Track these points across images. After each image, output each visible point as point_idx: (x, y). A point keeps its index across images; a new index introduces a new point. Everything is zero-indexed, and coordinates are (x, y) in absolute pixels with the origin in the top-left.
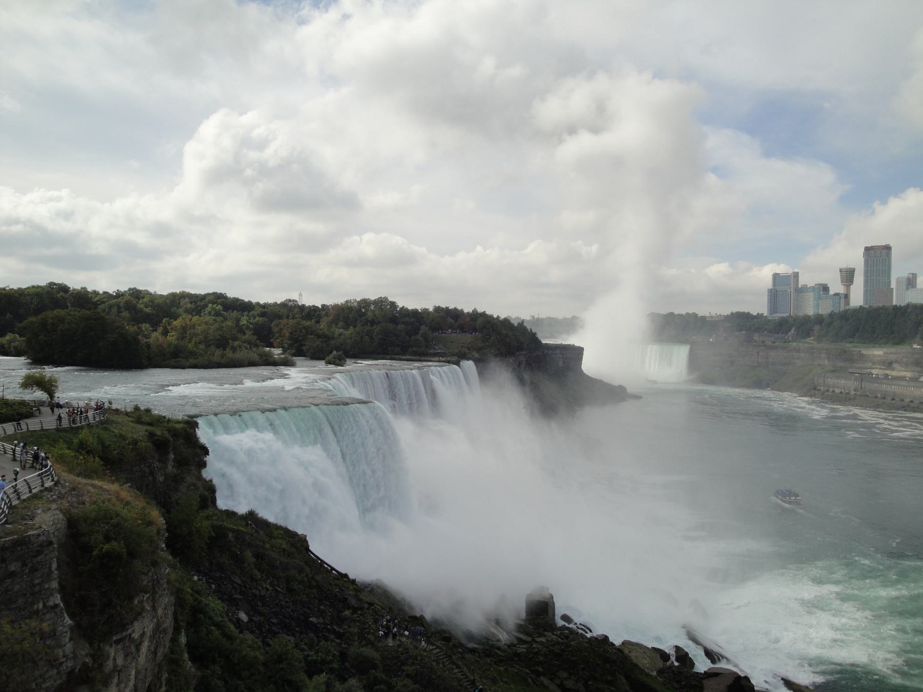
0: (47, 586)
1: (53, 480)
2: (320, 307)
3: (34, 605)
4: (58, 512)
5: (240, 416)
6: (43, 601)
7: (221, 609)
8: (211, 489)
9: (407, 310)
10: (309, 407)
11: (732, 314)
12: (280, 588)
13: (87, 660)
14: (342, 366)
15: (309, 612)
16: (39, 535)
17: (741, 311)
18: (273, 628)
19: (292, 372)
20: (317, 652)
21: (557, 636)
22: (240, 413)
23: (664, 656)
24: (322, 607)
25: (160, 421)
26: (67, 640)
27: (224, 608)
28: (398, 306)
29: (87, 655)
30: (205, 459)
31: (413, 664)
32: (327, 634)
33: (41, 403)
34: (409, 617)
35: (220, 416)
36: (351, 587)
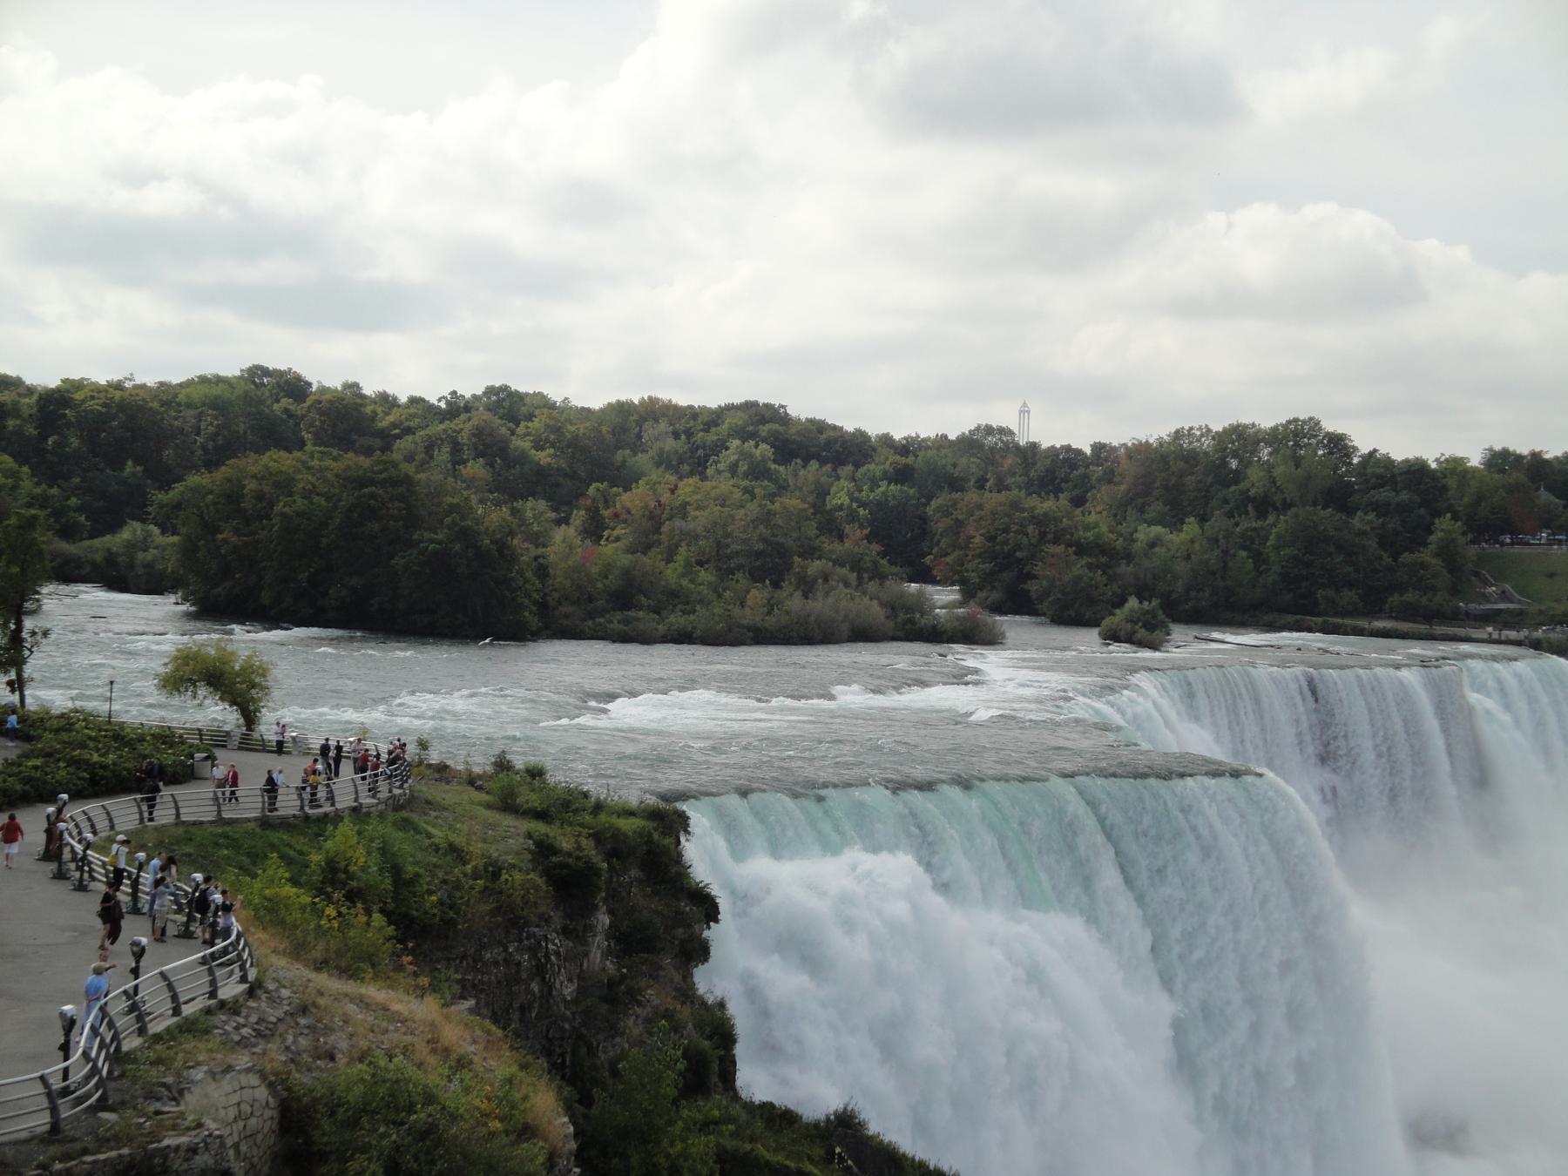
2: (1088, 451)
4: (254, 1080)
5: (820, 799)
8: (724, 1036)
9: (1388, 462)
14: (1154, 647)
16: (193, 1150)
19: (990, 662)
22: (823, 792)
28: (1355, 449)
30: (706, 934)
33: (220, 739)
35: (753, 797)
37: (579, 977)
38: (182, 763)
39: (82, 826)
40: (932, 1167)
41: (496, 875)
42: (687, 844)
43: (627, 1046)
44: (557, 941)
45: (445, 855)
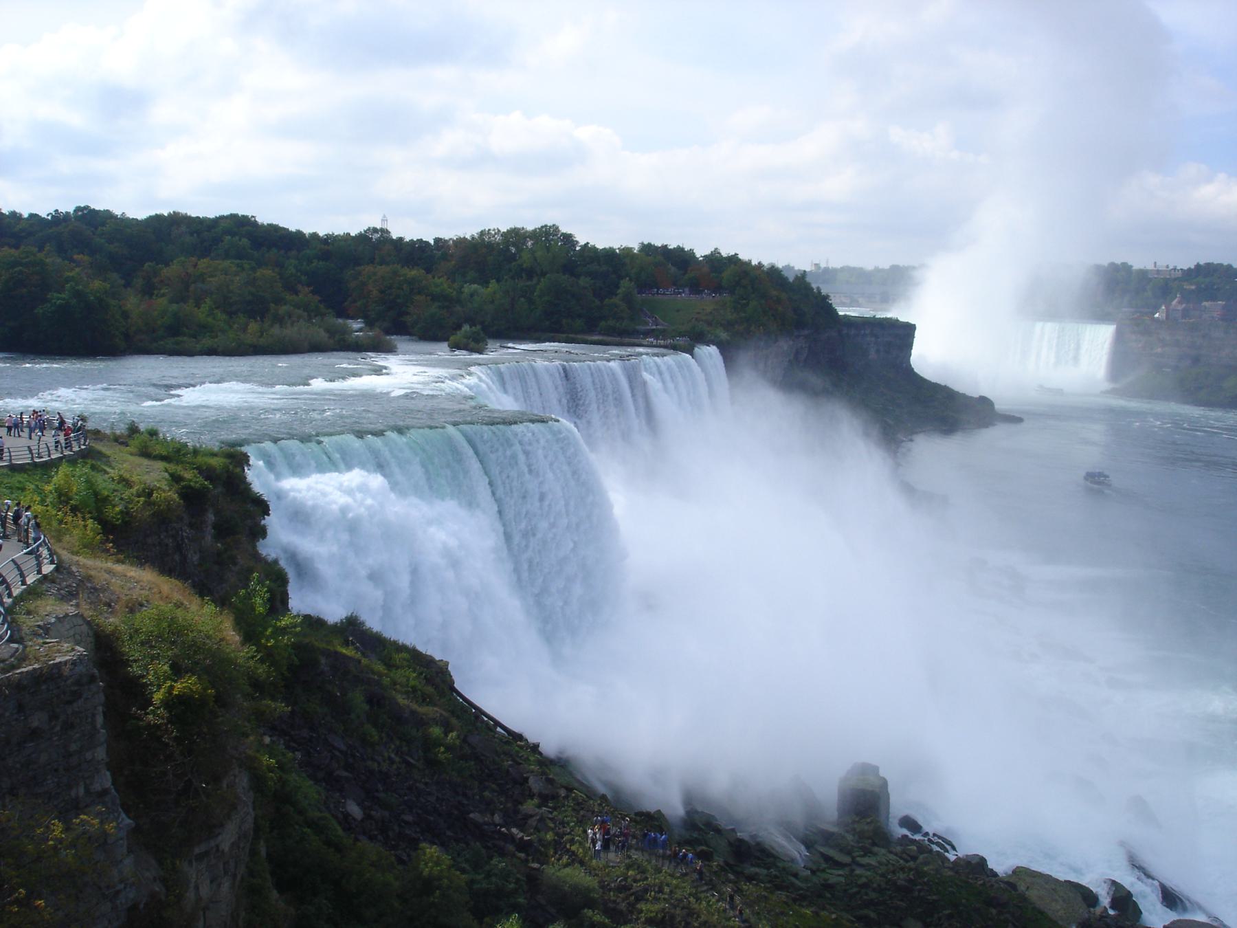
0: (88, 756)
1: (52, 562)
2: (432, 242)
4: (80, 622)
5: (319, 443)
7: (317, 797)
8: (277, 581)
9: (594, 248)
11: (1198, 266)
12: (413, 759)
13: (157, 889)
14: (481, 353)
16: (74, 663)
17: (1215, 263)
18: (408, 832)
20: (489, 875)
21: (896, 854)
22: (322, 439)
23: (1089, 898)
24: (487, 794)
25: (176, 454)
27: (320, 795)
28: (577, 242)
30: (263, 522)
31: (656, 899)
32: (502, 843)
34: (636, 814)
36: (532, 758)
37: (200, 552)
40: (400, 642)
41: (150, 494)
42: (248, 472)
43: (229, 589)
44: (187, 531)
45: (118, 483)
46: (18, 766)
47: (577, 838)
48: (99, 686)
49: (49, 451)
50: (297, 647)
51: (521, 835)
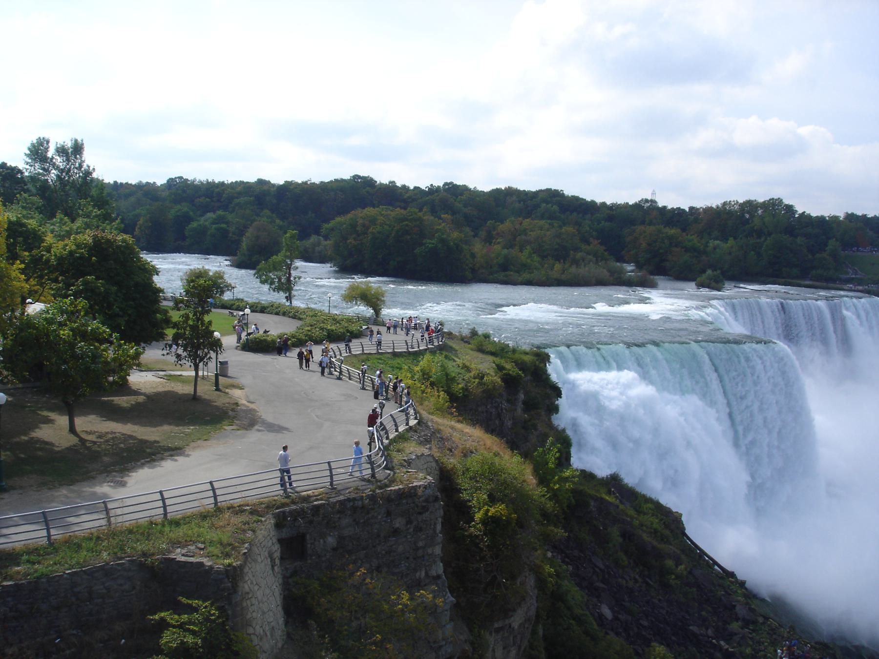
0: (430, 551)
1: (416, 418)
2: (687, 210)
3: (417, 572)
5: (599, 349)
6: (426, 569)
7: (581, 599)
8: (564, 443)
9: (809, 216)
10: (689, 343)
13: (467, 648)
14: (719, 291)
15: (689, 617)
16: (425, 487)
18: (644, 633)
24: (704, 613)
25: (500, 351)
26: (448, 619)
28: (796, 211)
29: (466, 641)
30: (557, 402)
32: (712, 651)
33: (367, 321)
34: (816, 643)
35: (573, 348)
36: (739, 591)
38: (358, 330)
39: (336, 354)
41: (482, 378)
45: (462, 369)
46: (384, 552)
47: (769, 655)
48: (441, 505)
49: (419, 345)
50: (574, 492)
51: (727, 647)
